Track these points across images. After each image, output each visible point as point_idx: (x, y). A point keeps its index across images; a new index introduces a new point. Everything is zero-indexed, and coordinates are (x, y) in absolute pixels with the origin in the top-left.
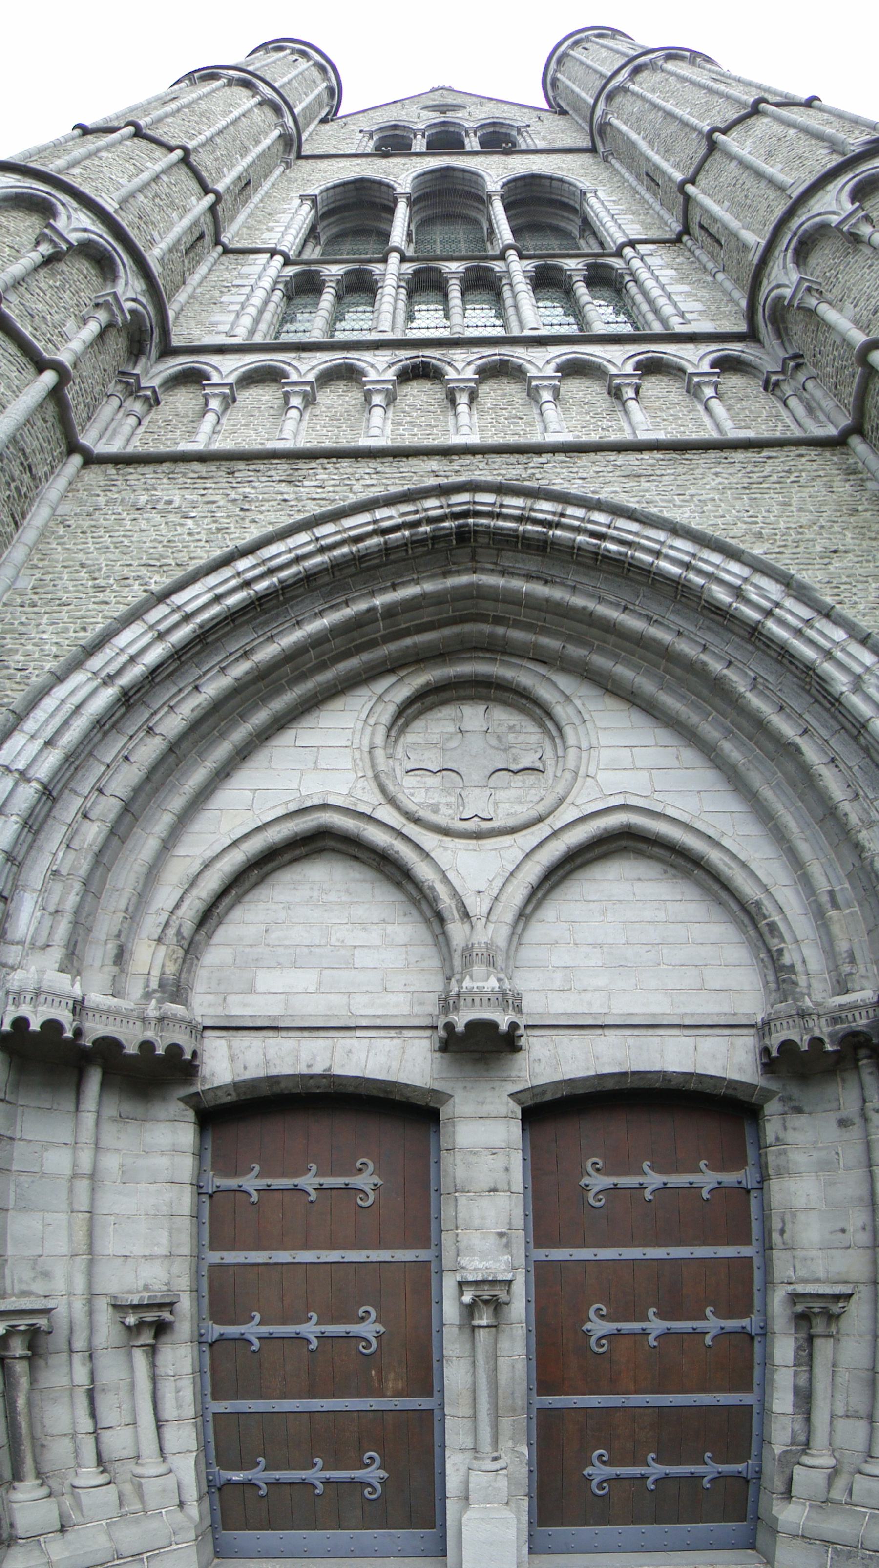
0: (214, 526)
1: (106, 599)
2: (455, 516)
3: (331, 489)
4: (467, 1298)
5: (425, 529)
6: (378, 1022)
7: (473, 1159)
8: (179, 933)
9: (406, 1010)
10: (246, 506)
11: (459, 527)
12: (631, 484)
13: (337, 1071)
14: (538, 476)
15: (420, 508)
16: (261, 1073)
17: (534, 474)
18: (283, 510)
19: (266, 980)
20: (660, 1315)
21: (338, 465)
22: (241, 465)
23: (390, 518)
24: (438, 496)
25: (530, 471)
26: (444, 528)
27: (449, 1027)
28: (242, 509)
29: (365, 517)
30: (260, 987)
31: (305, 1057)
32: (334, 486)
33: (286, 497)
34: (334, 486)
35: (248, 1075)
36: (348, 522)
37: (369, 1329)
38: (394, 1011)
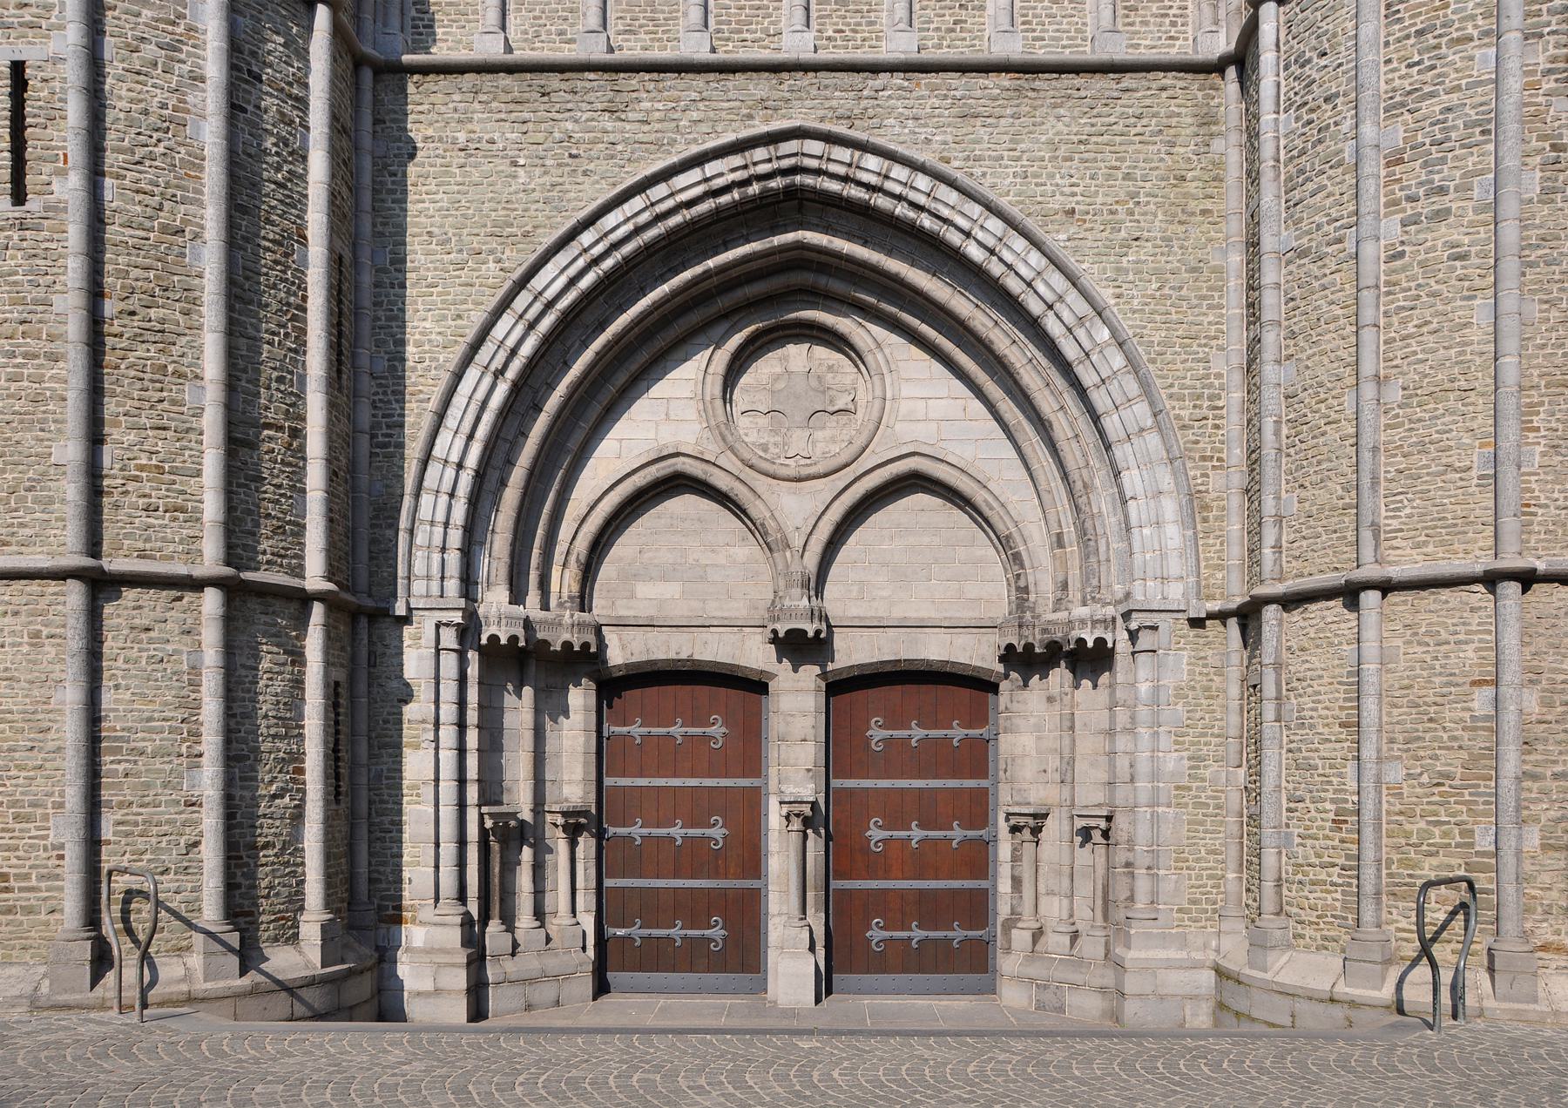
0: (547, 179)
1: (469, 280)
2: (784, 172)
3: (658, 126)
4: (784, 812)
5: (754, 189)
6: (726, 623)
7: (790, 719)
8: (578, 560)
9: (744, 613)
10: (574, 152)
11: (786, 187)
12: (964, 131)
13: (696, 657)
14: (871, 112)
15: (749, 161)
16: (644, 658)
17: (866, 109)
18: (612, 157)
19: (644, 590)
20: (921, 826)
21: (661, 85)
22: (554, 81)
23: (721, 175)
24: (766, 144)
25: (864, 103)
26: (772, 189)
27: (775, 632)
28: (571, 156)
29: (694, 175)
30: (639, 595)
31: (674, 647)
32: (660, 121)
33: (612, 137)
34: (660, 121)
35: (634, 660)
36: (681, 181)
37: (717, 832)
38: (737, 614)
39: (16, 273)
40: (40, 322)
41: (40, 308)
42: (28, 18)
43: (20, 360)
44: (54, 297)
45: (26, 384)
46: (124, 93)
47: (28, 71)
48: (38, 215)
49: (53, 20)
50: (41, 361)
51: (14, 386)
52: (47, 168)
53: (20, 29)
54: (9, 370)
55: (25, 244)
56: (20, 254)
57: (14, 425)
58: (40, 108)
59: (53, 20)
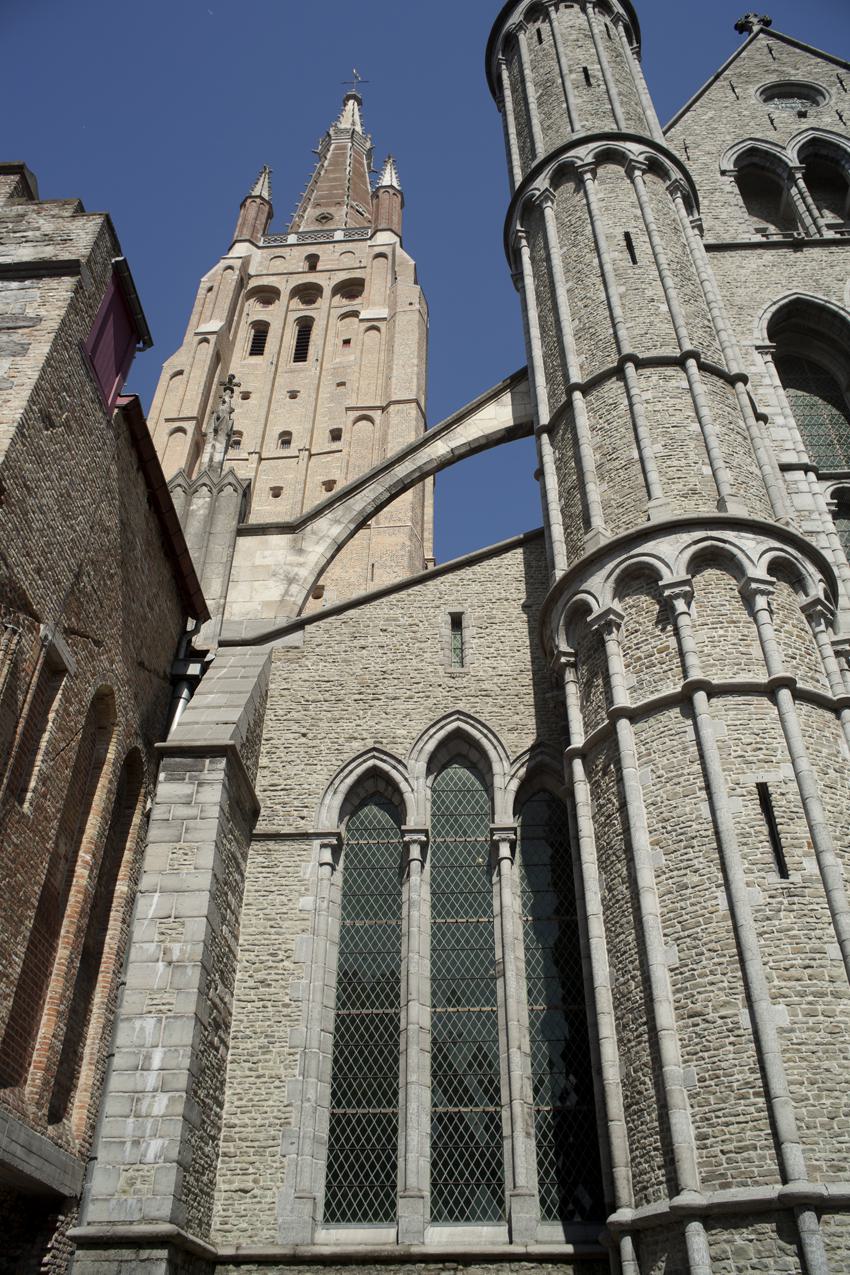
39: (793, 929)
40: (822, 966)
41: (818, 956)
42: (762, 757)
43: (811, 998)
44: (826, 946)
45: (822, 1018)
46: (828, 800)
47: (770, 789)
48: (799, 885)
49: (779, 757)
50: (829, 998)
51: (811, 1020)
52: (799, 852)
53: (758, 764)
54: (803, 1006)
55: (795, 907)
56: (792, 915)
57: (820, 1054)
58: (785, 812)
59: (779, 757)
